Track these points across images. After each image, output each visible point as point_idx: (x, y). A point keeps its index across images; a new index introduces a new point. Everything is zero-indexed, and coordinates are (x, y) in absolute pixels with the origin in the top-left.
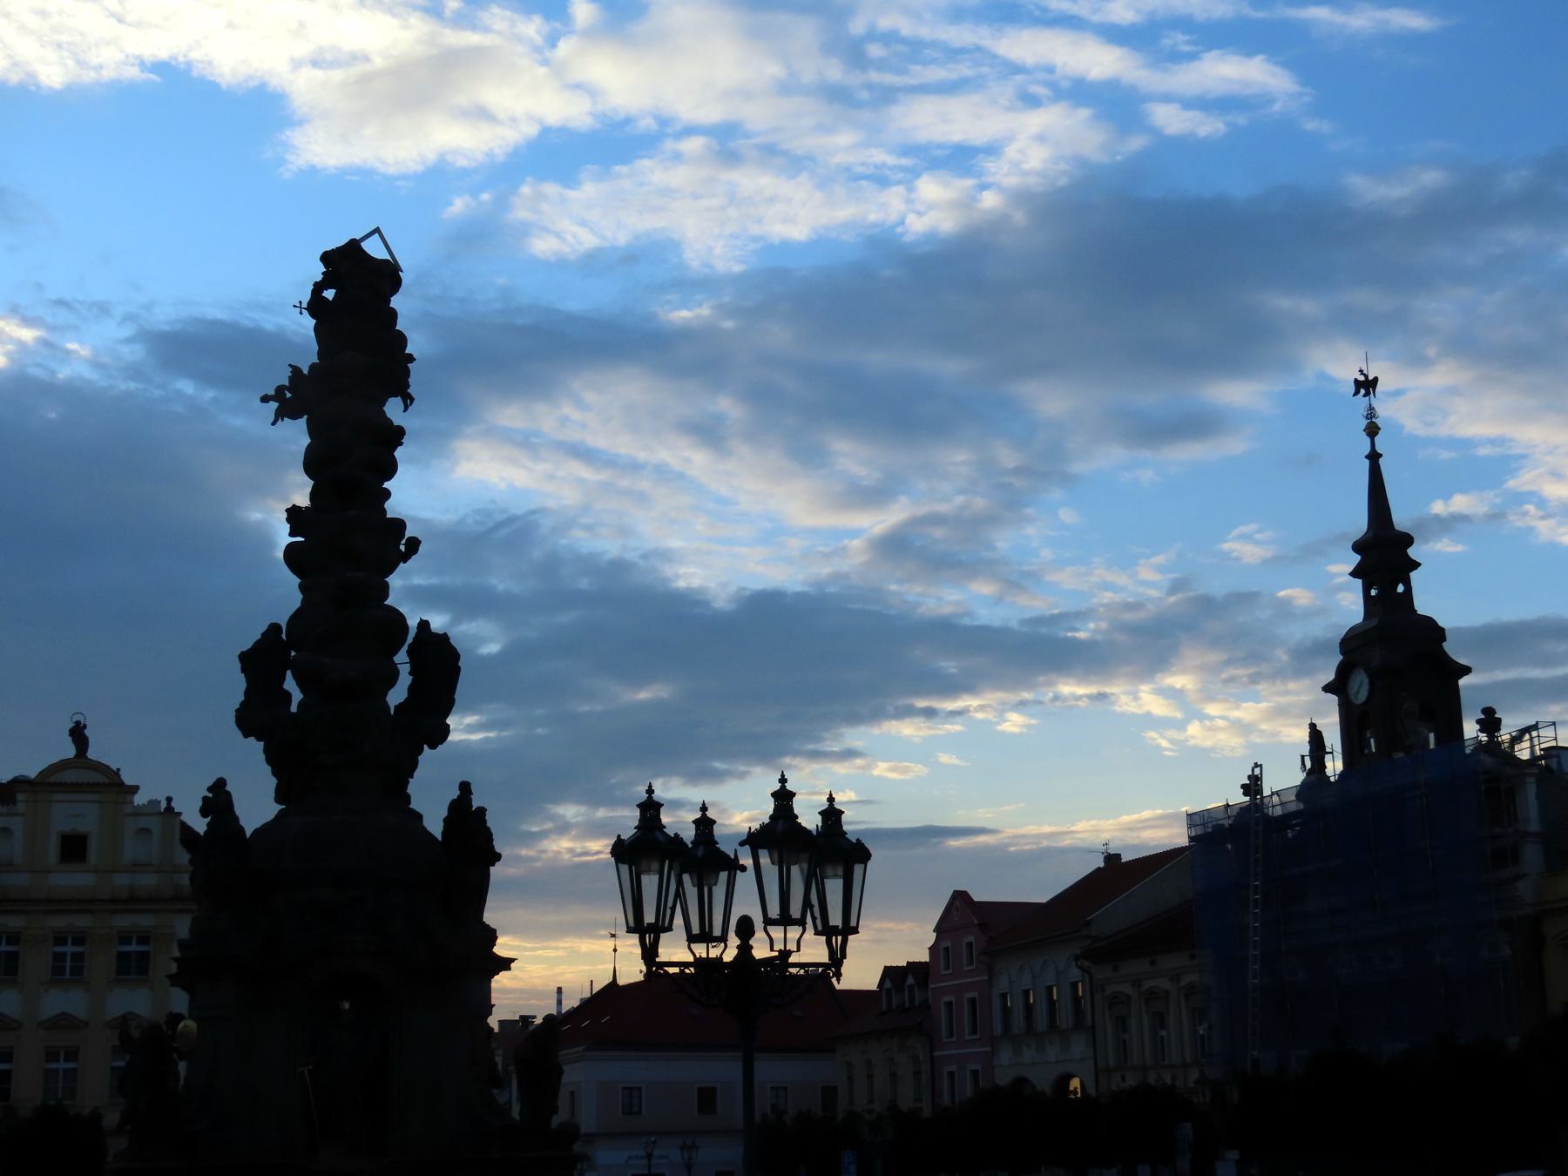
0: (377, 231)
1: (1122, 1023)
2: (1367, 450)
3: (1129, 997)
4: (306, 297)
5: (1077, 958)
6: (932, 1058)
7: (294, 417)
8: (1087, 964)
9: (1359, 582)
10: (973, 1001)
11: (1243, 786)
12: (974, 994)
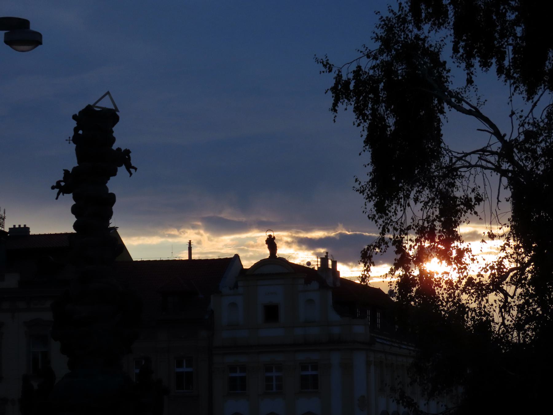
0: (108, 93)
4: (71, 134)
7: (68, 193)
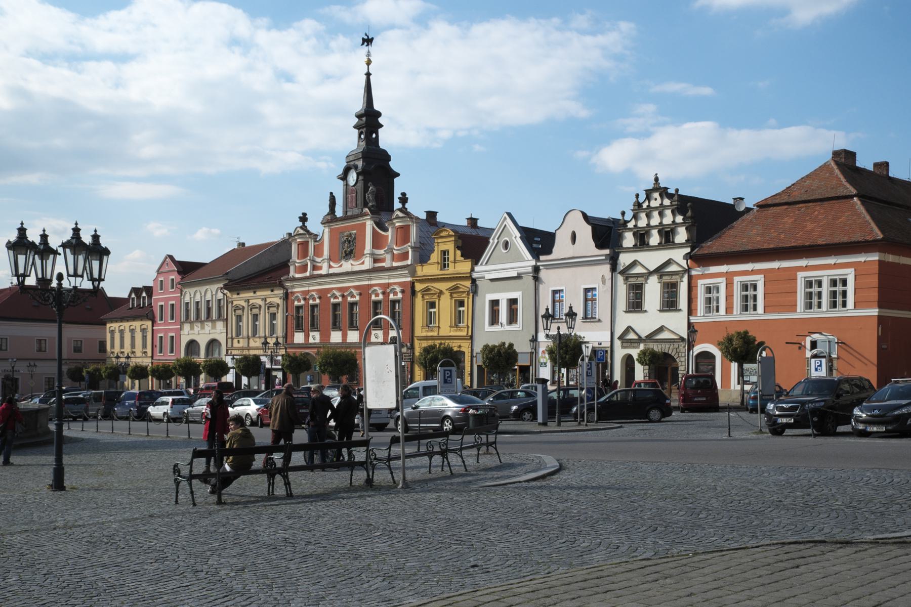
1: (239, 318)
2: (366, 71)
3: (243, 307)
5: (221, 288)
6: (153, 330)
8: (226, 291)
9: (356, 131)
10: (172, 305)
11: (300, 218)
12: (173, 302)
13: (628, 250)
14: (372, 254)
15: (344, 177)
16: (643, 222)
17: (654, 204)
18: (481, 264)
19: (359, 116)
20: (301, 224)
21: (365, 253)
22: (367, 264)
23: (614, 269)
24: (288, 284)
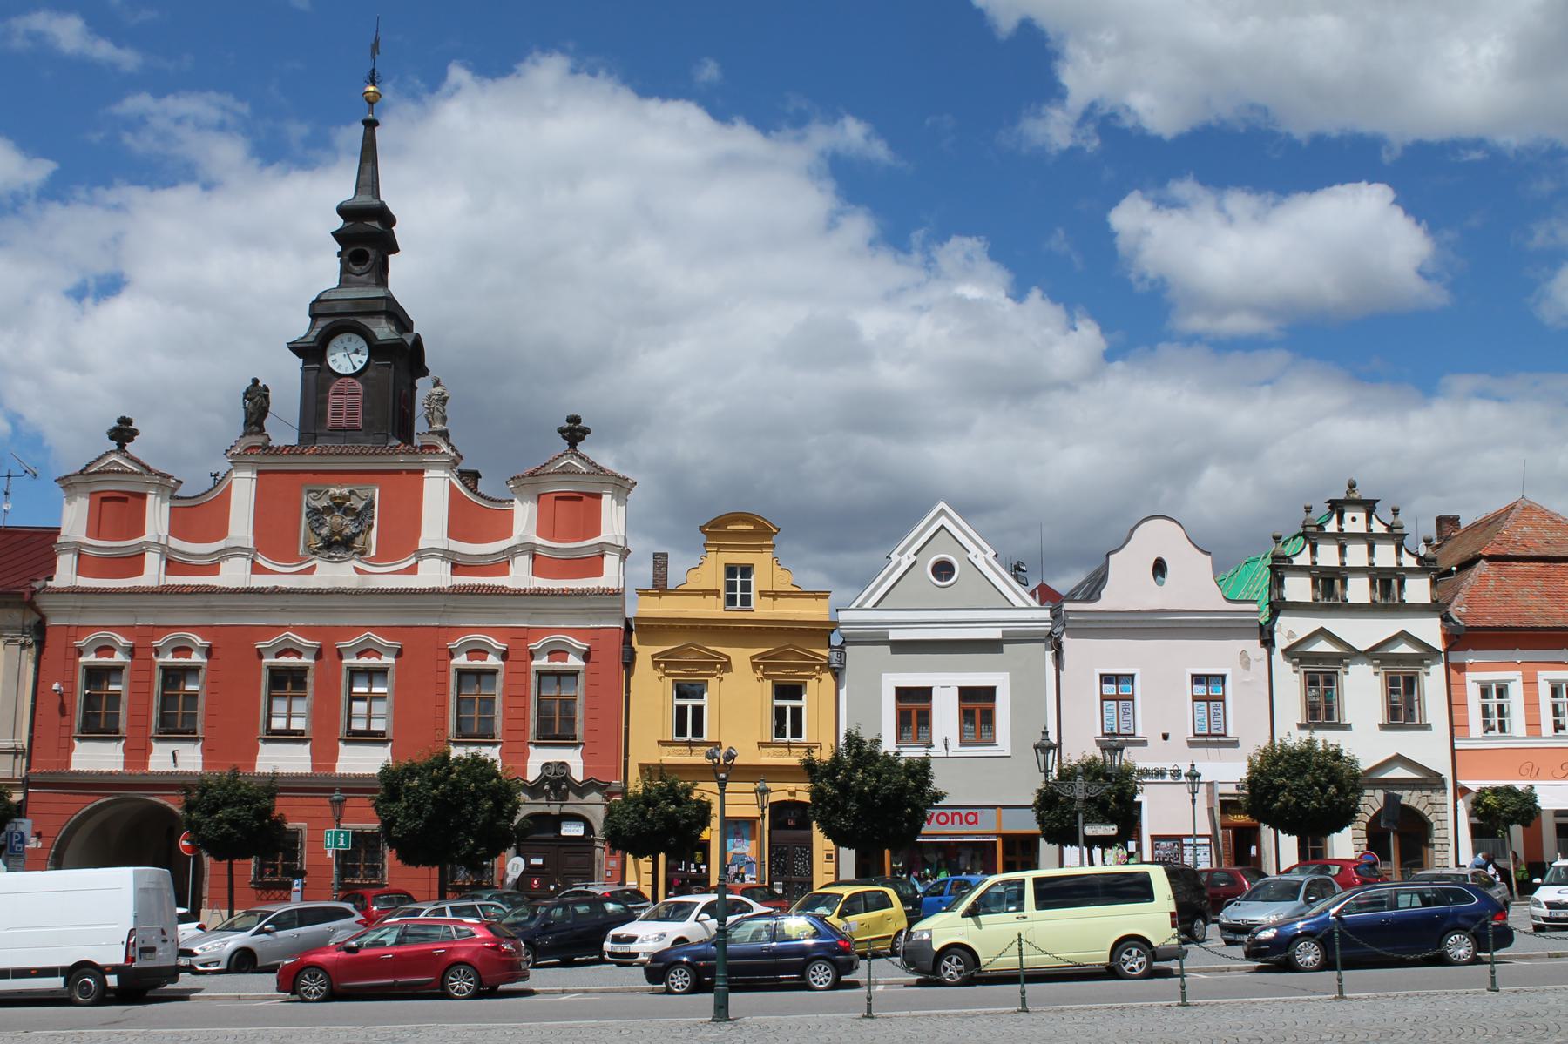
13: (1299, 608)
14: (446, 555)
15: (311, 352)
16: (1328, 556)
17: (1349, 527)
18: (859, 608)
19: (343, 211)
20: (113, 445)
21: (421, 546)
22: (433, 574)
23: (1268, 643)
24: (44, 602)
